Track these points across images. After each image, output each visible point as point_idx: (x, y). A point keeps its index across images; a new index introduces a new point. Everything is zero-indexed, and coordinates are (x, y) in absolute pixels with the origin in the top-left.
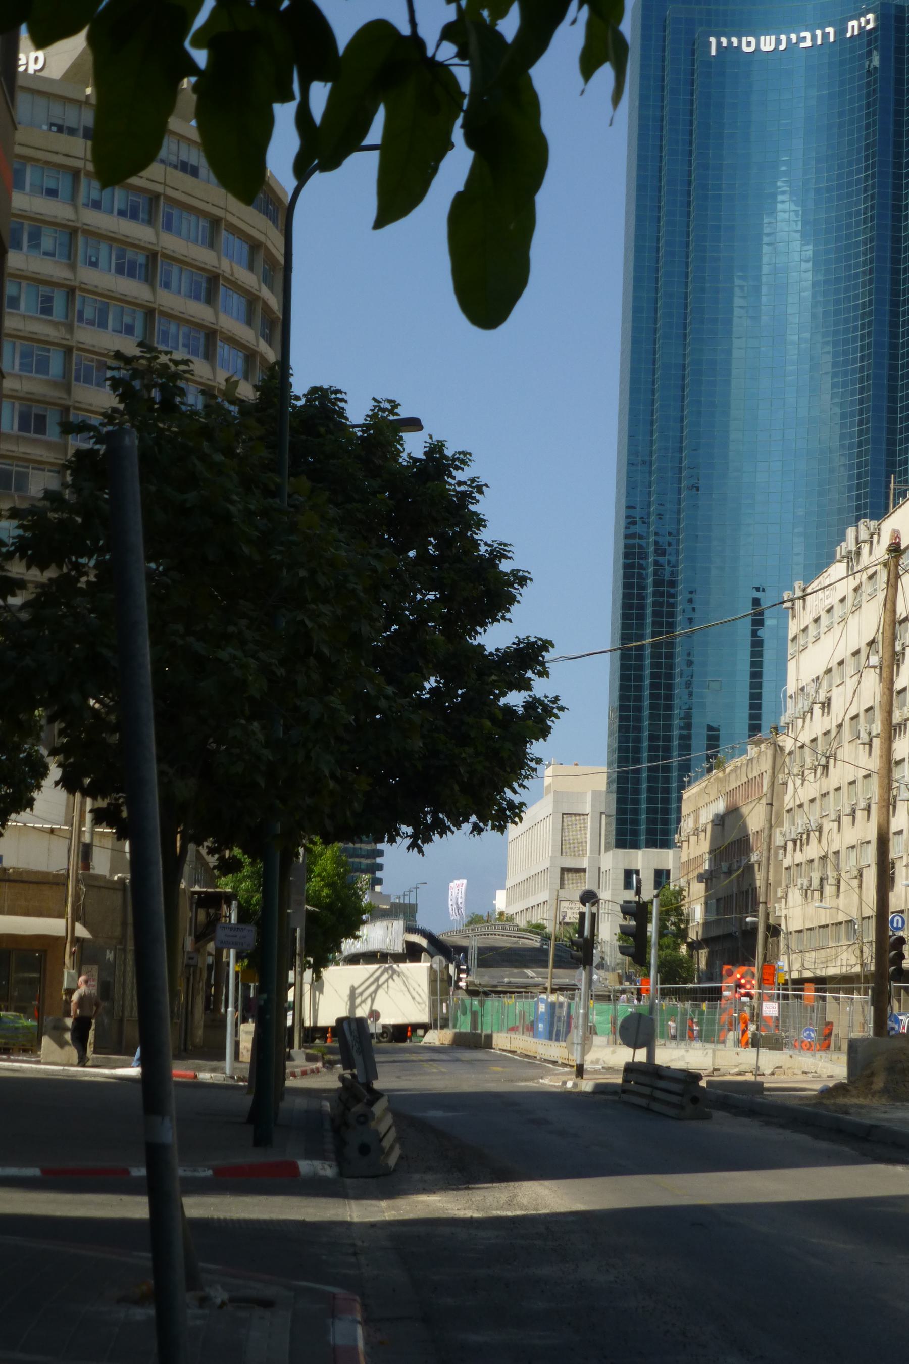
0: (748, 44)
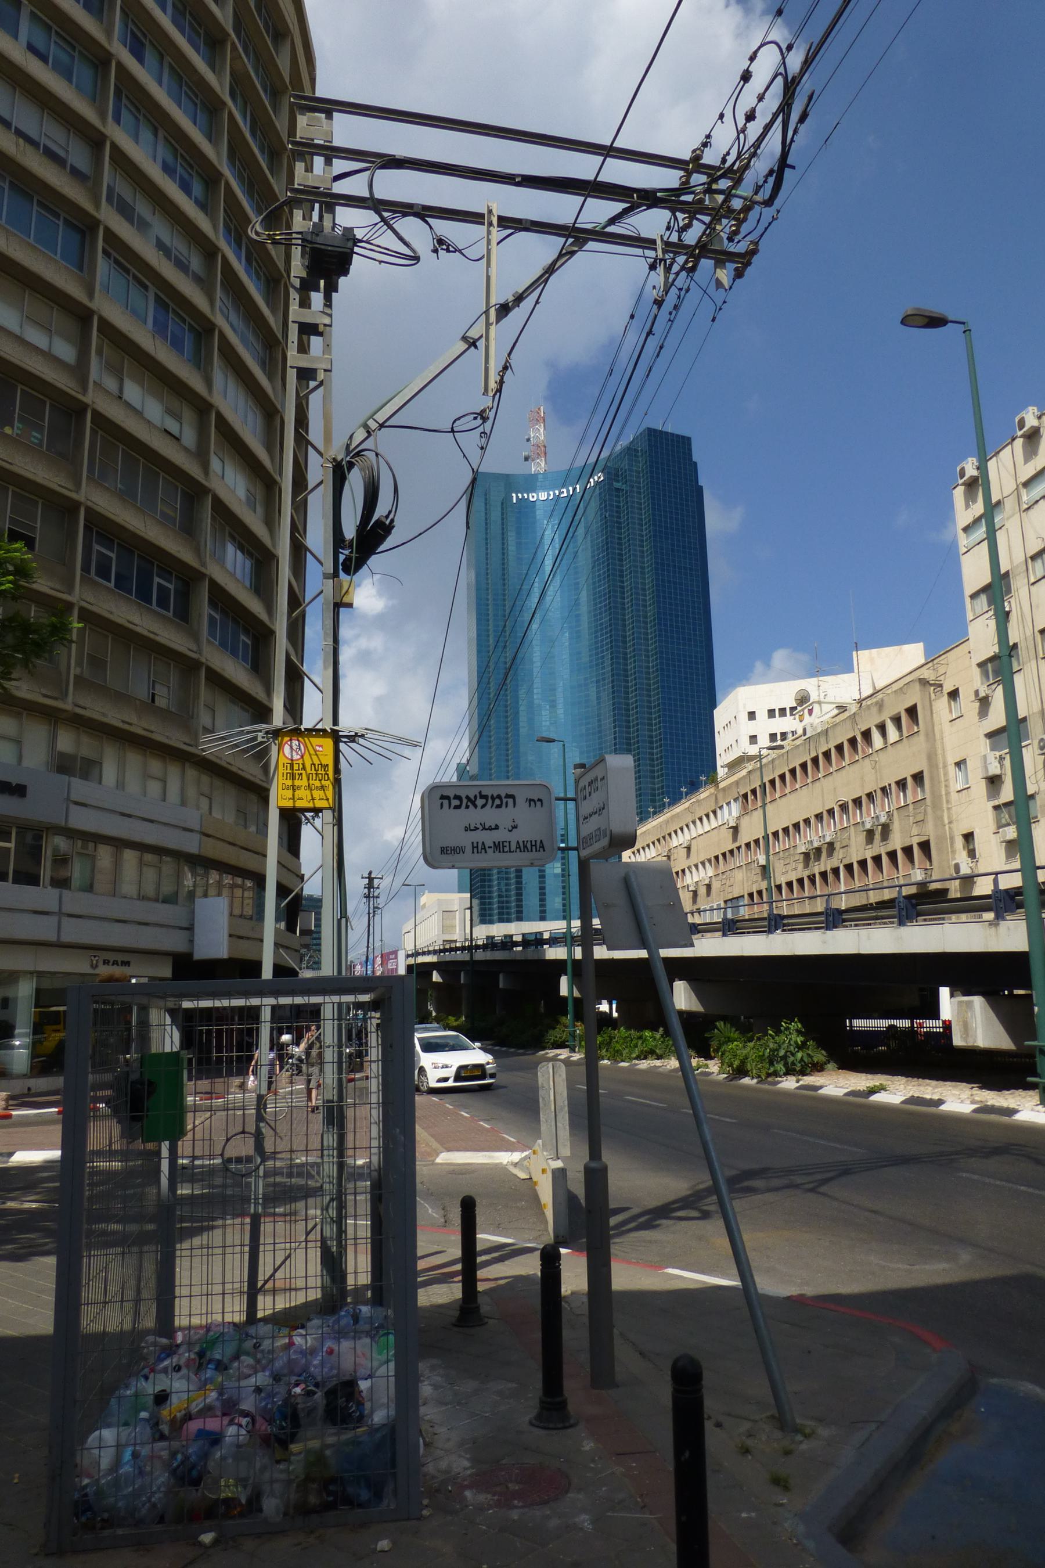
0: (532, 497)
